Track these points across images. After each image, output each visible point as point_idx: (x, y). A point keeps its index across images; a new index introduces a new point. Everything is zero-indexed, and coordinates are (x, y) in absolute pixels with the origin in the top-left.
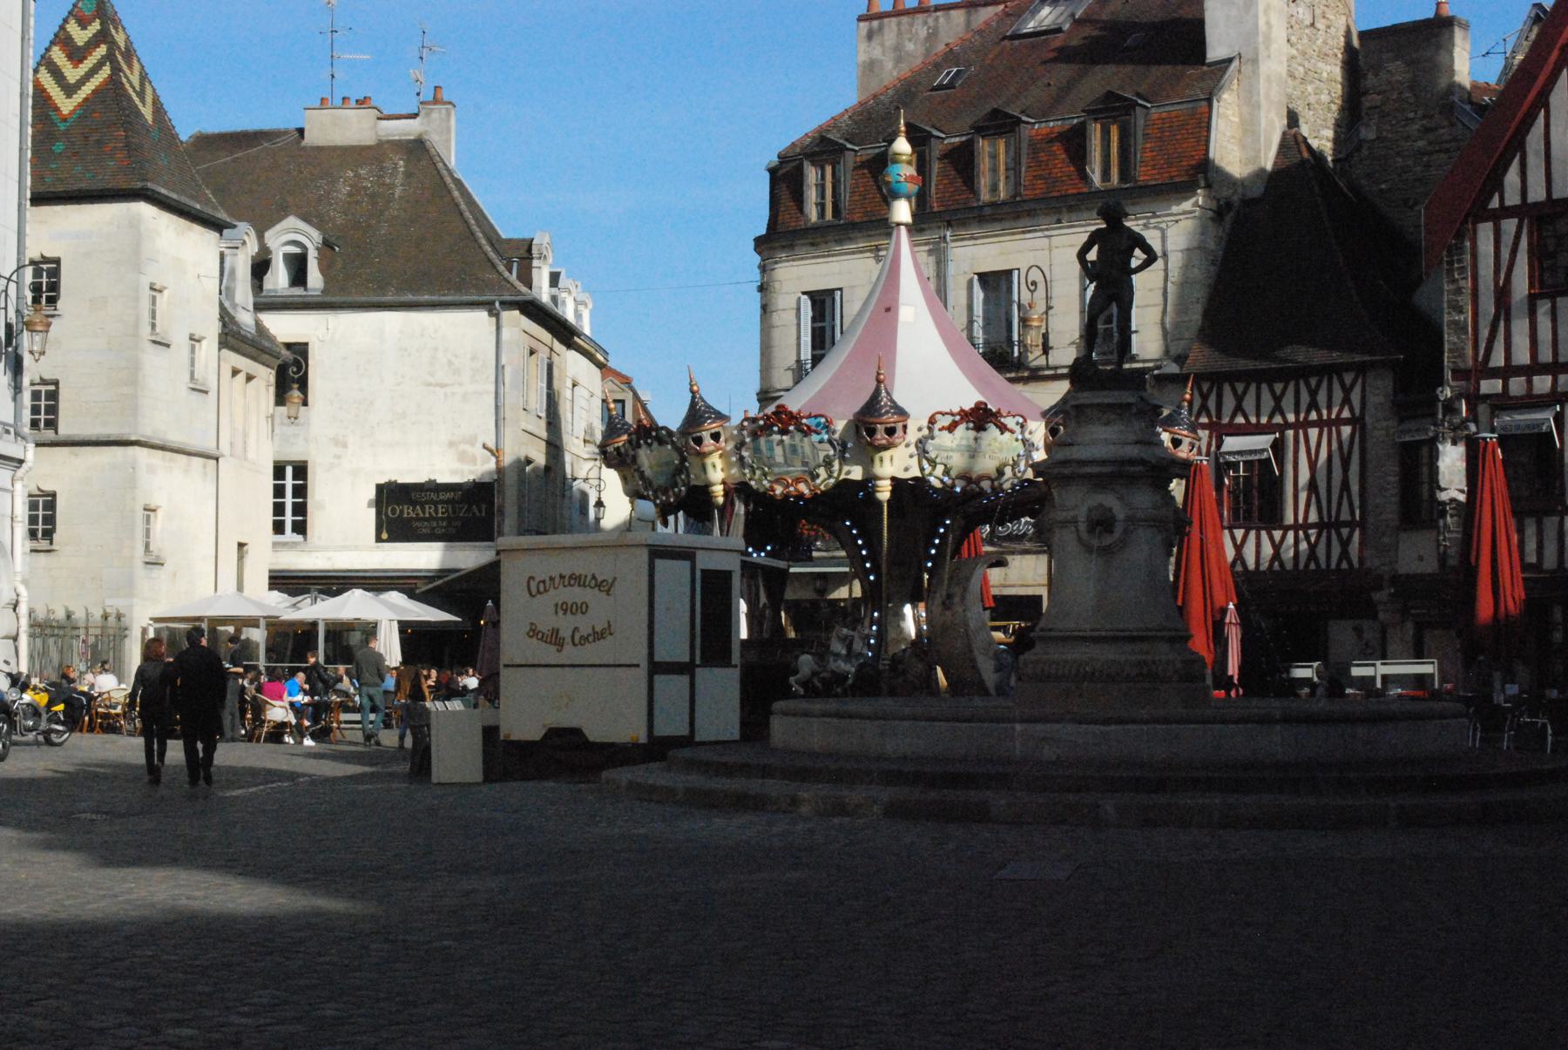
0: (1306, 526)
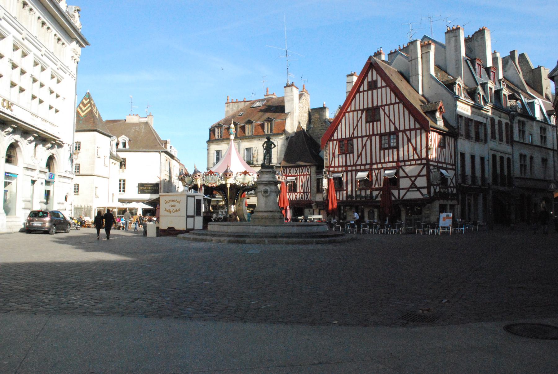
0: (301, 193)
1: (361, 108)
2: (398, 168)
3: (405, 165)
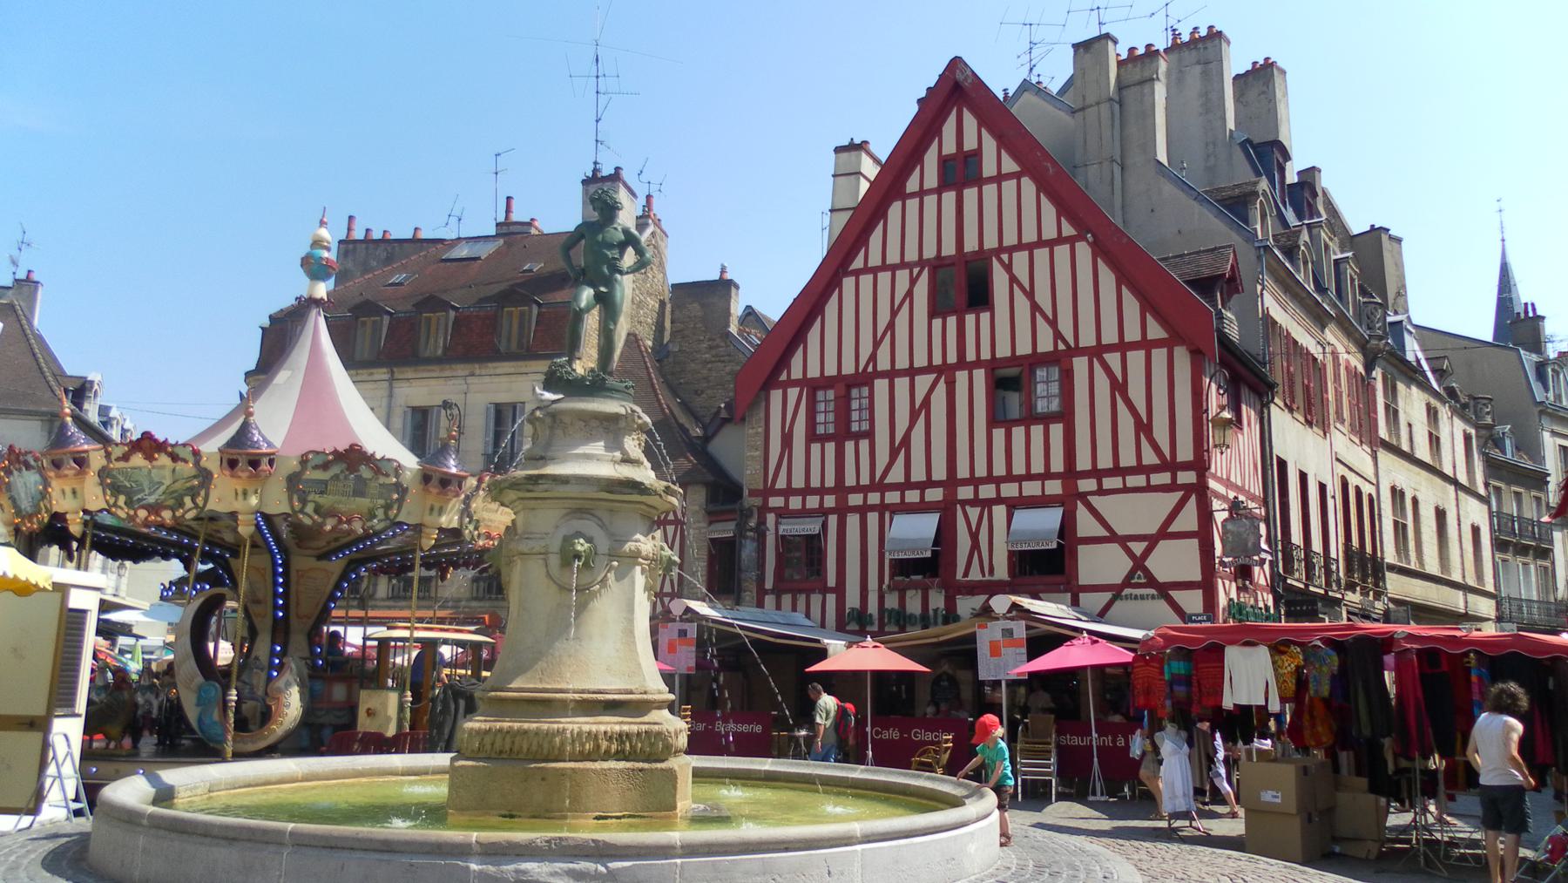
1: (912, 255)
2: (1069, 500)
3: (1101, 492)
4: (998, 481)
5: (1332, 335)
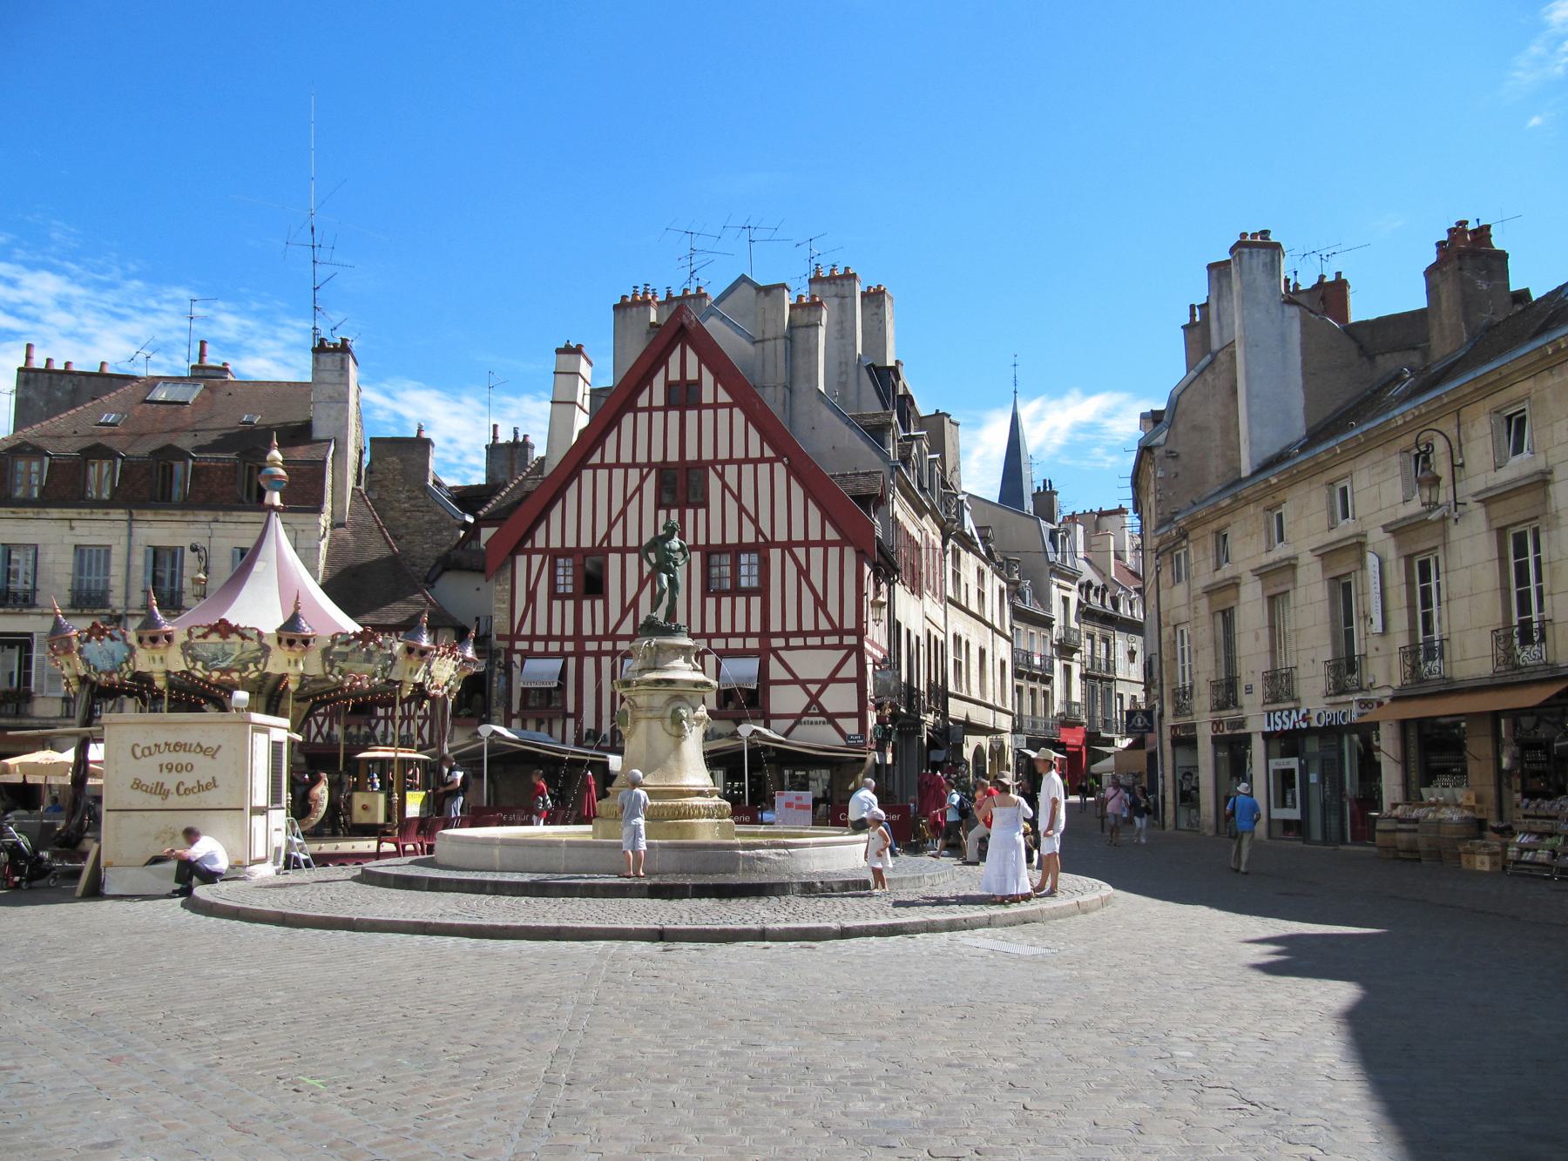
1: (642, 458)
2: (764, 653)
3: (788, 648)
4: (709, 637)
5: (927, 523)
